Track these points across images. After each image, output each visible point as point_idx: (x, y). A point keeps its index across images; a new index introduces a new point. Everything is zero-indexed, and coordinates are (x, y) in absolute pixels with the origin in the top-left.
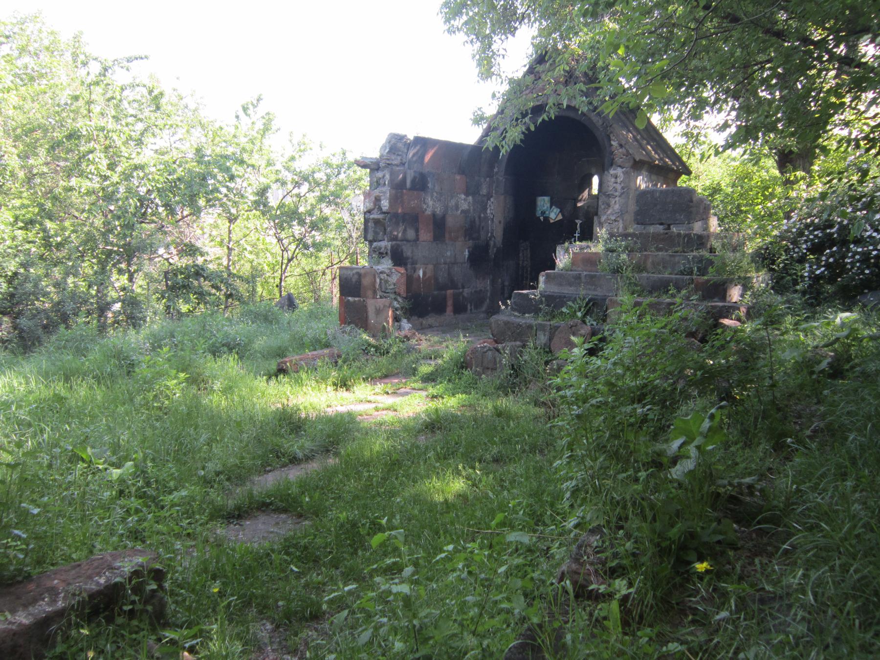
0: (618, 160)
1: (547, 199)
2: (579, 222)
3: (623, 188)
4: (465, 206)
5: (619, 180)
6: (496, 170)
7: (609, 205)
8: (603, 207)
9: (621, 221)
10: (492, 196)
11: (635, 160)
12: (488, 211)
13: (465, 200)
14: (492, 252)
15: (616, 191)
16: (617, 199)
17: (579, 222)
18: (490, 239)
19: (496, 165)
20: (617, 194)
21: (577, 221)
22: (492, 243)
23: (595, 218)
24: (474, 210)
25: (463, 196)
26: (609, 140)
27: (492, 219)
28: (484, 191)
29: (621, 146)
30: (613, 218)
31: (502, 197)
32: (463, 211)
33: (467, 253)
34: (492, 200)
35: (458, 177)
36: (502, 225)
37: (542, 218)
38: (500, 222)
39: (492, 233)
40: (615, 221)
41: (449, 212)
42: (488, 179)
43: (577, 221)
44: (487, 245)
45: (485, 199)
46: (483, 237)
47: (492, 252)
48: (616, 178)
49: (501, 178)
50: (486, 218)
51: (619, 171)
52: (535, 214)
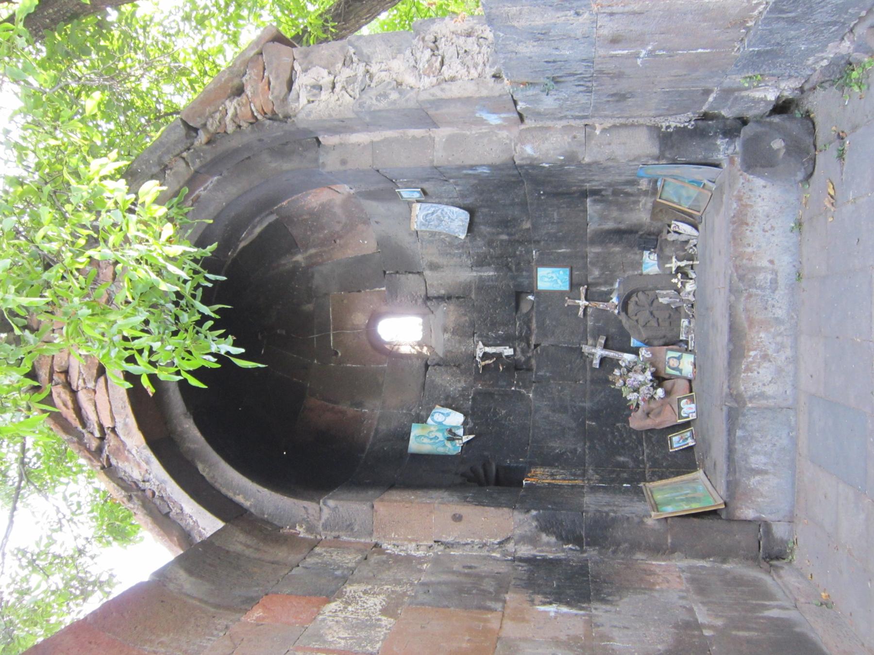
1: (416, 430)
2: (481, 349)
4: (375, 603)
6: (301, 531)
8: (394, 96)
9: (435, 28)
12: (420, 553)
14: (549, 547)
15: (351, 80)
16: (374, 69)
17: (481, 349)
19: (287, 530)
21: (479, 353)
22: (525, 551)
24: (398, 582)
25: (333, 606)
27: (448, 545)
28: (350, 559)
29: (239, 91)
30: (428, 53)
32: (385, 611)
33: (552, 609)
34: (385, 546)
35: (257, 613)
36: (469, 511)
37: (466, 439)
38: (457, 518)
40: (435, 50)
42: (317, 550)
43: (479, 353)
44: (530, 561)
45: (374, 558)
46: (503, 568)
47: (549, 547)
49: (326, 513)
50: (436, 561)
51: (302, 80)
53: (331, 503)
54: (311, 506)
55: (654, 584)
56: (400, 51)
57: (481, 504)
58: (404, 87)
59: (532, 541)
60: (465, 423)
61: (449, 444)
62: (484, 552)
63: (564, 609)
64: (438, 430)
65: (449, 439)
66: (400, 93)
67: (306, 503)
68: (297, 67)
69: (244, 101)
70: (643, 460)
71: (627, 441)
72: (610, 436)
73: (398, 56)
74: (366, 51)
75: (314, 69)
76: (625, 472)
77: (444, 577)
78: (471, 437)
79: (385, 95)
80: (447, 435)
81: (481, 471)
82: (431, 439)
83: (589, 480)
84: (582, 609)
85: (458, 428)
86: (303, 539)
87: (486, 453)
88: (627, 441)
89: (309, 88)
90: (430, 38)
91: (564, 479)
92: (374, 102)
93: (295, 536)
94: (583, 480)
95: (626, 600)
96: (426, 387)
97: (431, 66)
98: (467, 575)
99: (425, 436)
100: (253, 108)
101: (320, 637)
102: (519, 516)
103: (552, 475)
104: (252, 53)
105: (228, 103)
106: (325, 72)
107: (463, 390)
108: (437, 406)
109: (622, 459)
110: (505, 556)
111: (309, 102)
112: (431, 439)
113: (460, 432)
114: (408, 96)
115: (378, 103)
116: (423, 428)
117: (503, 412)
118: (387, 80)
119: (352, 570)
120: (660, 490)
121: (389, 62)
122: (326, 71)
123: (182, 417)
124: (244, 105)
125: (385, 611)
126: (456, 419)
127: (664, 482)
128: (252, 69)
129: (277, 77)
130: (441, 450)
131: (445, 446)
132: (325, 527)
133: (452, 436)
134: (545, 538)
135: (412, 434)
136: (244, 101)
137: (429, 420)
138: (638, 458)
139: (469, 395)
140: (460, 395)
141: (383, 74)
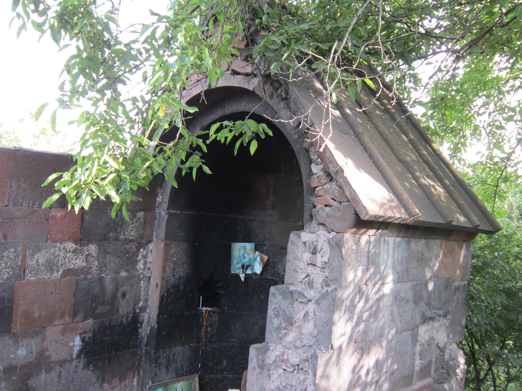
0: (322, 212)
3: (326, 283)
5: (320, 260)
6: (159, 199)
7: (290, 321)
10: (150, 241)
11: (357, 215)
12: (141, 265)
13: (75, 251)
15: (311, 284)
16: (311, 307)
18: (143, 309)
20: (311, 294)
23: (253, 350)
25: (71, 246)
26: (311, 162)
27: (150, 278)
30: (294, 359)
31: (162, 245)
32: (68, 272)
33: (77, 343)
34: (151, 246)
37: (242, 277)
38: (157, 284)
39: (146, 300)
41: (30, 277)
44: (135, 322)
48: (314, 253)
49: (163, 213)
52: (229, 270)
53: (166, 217)
54: (165, 206)
55: (109, 382)
56: (319, 332)
57: (162, 298)
58: (284, 331)
59: (149, 322)
60: (255, 274)
61: (240, 265)
62: (142, 298)
63: (77, 349)
64: (250, 259)
65: (243, 266)
66: (277, 328)
67: (167, 202)
68: (333, 234)
69: (322, 181)
70: (224, 374)
71: (238, 366)
72: (242, 357)
73: (316, 330)
74: (324, 302)
75: (329, 250)
76: (213, 364)
77: (109, 287)
78: (243, 279)
79: (277, 315)
80: (246, 265)
81: (219, 285)
82: (243, 255)
83: (206, 346)
84: (78, 356)
85: (253, 269)
86: (156, 201)
87: (232, 287)
88: (238, 366)
89: (315, 244)
90: (306, 366)
91: (206, 332)
92: (274, 306)
93: (157, 195)
94: (206, 342)
95: (90, 373)
96: (282, 250)
97: (283, 361)
98: (114, 297)
99: (245, 252)
100: (318, 188)
101: (38, 249)
102: (155, 317)
103: (211, 325)
104: (347, 194)
105: (321, 166)
106: (325, 259)
107: (278, 273)
108: (266, 258)
109: (225, 363)
110: (140, 308)
111: (304, 243)
112: (243, 255)
113: (249, 272)
114: (274, 334)
115: (272, 309)
116: (251, 250)
117: (263, 297)
118: (296, 317)
119: (117, 239)
120: (190, 385)
121: (313, 320)
122: (327, 260)
123: (201, 125)
124: (319, 180)
125: (64, 271)
126: (258, 269)
127: (197, 386)
128: (339, 191)
129: (328, 216)
130: (234, 261)
131: (238, 263)
132: (160, 213)
133: (244, 267)
134: (149, 328)
135: (246, 244)
136: (322, 181)
137: (257, 253)
138: (225, 371)
139: (275, 277)
140: (275, 272)
141: (302, 314)
